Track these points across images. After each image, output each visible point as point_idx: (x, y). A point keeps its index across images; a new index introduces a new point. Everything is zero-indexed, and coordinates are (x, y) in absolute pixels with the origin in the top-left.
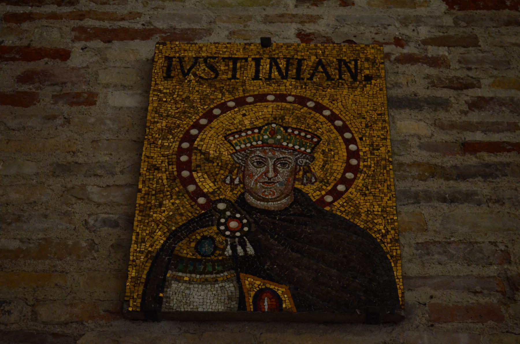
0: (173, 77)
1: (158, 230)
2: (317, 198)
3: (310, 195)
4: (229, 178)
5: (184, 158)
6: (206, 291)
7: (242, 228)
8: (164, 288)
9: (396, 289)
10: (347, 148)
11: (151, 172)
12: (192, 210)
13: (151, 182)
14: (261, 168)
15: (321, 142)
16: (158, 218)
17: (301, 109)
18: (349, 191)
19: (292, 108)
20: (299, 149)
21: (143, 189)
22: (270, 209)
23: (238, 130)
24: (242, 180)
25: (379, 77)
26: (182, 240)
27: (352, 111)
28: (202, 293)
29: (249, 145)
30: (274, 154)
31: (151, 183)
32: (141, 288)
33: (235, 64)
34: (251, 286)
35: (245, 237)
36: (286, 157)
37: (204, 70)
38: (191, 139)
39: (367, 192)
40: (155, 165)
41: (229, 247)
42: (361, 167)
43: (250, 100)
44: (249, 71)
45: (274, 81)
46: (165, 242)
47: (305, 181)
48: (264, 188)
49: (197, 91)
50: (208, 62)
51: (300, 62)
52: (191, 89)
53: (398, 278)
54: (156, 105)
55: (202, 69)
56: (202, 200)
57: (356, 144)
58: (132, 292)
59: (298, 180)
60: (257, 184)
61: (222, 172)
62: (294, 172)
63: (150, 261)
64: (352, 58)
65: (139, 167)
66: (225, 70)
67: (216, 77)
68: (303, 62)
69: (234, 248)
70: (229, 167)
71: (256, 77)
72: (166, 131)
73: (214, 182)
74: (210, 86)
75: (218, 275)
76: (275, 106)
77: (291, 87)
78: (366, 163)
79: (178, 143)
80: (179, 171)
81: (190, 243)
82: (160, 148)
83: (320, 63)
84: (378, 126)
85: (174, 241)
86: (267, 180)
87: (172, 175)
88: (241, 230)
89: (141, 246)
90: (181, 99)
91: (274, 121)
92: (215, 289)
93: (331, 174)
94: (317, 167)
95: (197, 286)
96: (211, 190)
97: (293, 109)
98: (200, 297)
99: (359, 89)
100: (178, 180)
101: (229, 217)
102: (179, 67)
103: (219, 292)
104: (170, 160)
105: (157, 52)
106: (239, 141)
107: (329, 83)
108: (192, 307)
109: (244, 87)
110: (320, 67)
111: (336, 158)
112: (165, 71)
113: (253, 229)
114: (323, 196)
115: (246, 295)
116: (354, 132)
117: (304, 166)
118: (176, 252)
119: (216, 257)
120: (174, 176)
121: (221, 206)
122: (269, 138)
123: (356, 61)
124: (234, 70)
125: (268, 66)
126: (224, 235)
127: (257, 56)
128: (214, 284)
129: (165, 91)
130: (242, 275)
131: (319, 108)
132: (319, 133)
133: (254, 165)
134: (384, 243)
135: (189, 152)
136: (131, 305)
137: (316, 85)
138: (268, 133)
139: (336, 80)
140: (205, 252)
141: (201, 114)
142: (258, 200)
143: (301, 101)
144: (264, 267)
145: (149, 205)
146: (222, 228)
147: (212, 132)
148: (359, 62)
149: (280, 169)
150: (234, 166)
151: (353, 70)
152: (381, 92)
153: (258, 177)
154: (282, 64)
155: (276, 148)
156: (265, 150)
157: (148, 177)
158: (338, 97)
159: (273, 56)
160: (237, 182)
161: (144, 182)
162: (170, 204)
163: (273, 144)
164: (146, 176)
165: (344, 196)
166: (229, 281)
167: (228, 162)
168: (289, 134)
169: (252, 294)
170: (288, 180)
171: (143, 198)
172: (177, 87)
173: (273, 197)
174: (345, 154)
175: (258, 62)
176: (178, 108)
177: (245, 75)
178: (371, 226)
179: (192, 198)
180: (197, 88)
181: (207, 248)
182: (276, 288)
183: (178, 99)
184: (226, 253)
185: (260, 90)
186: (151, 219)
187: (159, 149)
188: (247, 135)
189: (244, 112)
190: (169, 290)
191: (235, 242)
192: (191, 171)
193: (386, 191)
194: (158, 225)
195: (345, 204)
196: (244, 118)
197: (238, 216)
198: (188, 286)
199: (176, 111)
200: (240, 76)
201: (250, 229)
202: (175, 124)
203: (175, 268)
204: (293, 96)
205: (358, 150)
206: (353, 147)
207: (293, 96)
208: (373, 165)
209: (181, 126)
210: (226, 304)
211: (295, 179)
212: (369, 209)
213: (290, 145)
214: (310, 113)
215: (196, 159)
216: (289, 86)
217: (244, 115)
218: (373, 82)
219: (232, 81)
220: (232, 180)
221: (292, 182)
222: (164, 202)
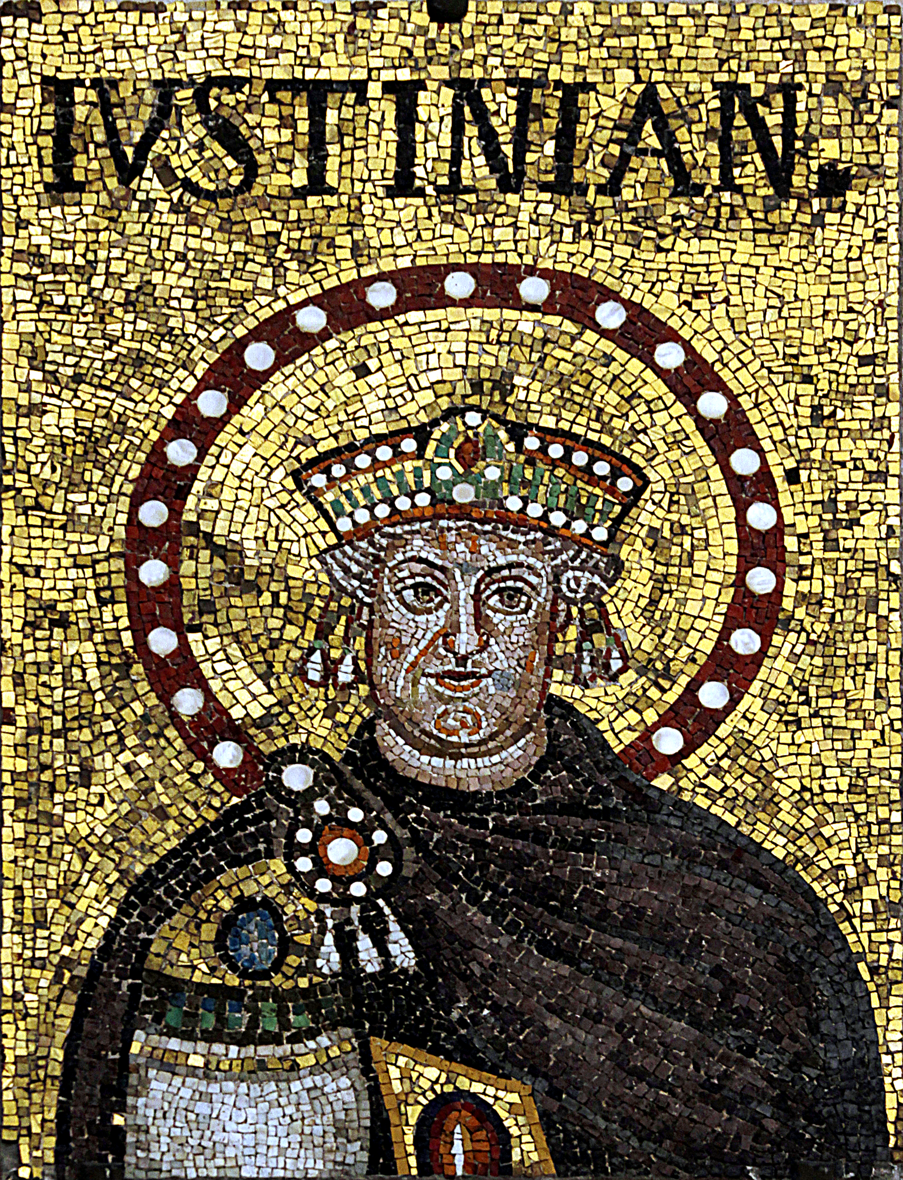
0: (80, 187)
2: (628, 737)
4: (317, 657)
5: (153, 572)
8: (124, 1095)
10: (741, 521)
11: (39, 634)
13: (44, 678)
14: (429, 611)
15: (646, 495)
18: (741, 707)
20: (567, 525)
23: (344, 440)
26: (170, 913)
29: (383, 511)
32: (53, 1097)
35: (381, 902)
39: (804, 711)
41: (329, 939)
42: (788, 604)
43: (382, 296)
45: (471, 198)
46: (116, 923)
49: (181, 257)
50: (213, 104)
53: (889, 1052)
56: (227, 754)
60: (415, 683)
61: (292, 632)
62: (549, 629)
66: (279, 145)
71: (403, 185)
75: (298, 1048)
76: (476, 324)
78: (804, 586)
79: (125, 503)
80: (140, 632)
81: (198, 927)
82: (63, 527)
83: (648, 104)
84: (858, 413)
87: (115, 649)
88: (367, 874)
90: (120, 296)
91: (474, 400)
92: (293, 1098)
96: (257, 712)
97: (545, 341)
101: (326, 819)
104: (104, 581)
106: (348, 494)
107: (684, 210)
108: (220, 1162)
110: (648, 126)
111: (699, 568)
115: (394, 1119)
116: (767, 445)
118: (154, 963)
121: (296, 777)
127: (404, 75)
129: (57, 257)
130: (377, 1043)
131: (642, 333)
132: (636, 454)
134: (849, 918)
136: (25, 1159)
137: (634, 222)
138: (452, 452)
139: (708, 191)
143: (576, 297)
144: (448, 1013)
145: (47, 776)
147: (246, 453)
148: (801, 95)
149: (497, 618)
152: (880, 250)
153: (422, 653)
155: (482, 522)
157: (30, 658)
158: (715, 278)
160: (345, 675)
165: (723, 730)
167: (312, 589)
169: (414, 1113)
172: (103, 236)
173: (475, 738)
174: (733, 546)
176: (114, 341)
179: (191, 746)
181: (257, 947)
182: (491, 1091)
186: (59, 831)
187: (59, 534)
190: (141, 1101)
191: (349, 922)
192: (181, 629)
195: (725, 763)
197: (355, 815)
201: (397, 867)
204: (545, 274)
205: (780, 528)
206: (761, 516)
207: (545, 274)
209: (132, 423)
212: (807, 782)
213: (535, 510)
214: (609, 359)
216: (530, 230)
218: (852, 197)
219: (312, 201)
220: (330, 668)
221: (542, 673)
222: (98, 763)
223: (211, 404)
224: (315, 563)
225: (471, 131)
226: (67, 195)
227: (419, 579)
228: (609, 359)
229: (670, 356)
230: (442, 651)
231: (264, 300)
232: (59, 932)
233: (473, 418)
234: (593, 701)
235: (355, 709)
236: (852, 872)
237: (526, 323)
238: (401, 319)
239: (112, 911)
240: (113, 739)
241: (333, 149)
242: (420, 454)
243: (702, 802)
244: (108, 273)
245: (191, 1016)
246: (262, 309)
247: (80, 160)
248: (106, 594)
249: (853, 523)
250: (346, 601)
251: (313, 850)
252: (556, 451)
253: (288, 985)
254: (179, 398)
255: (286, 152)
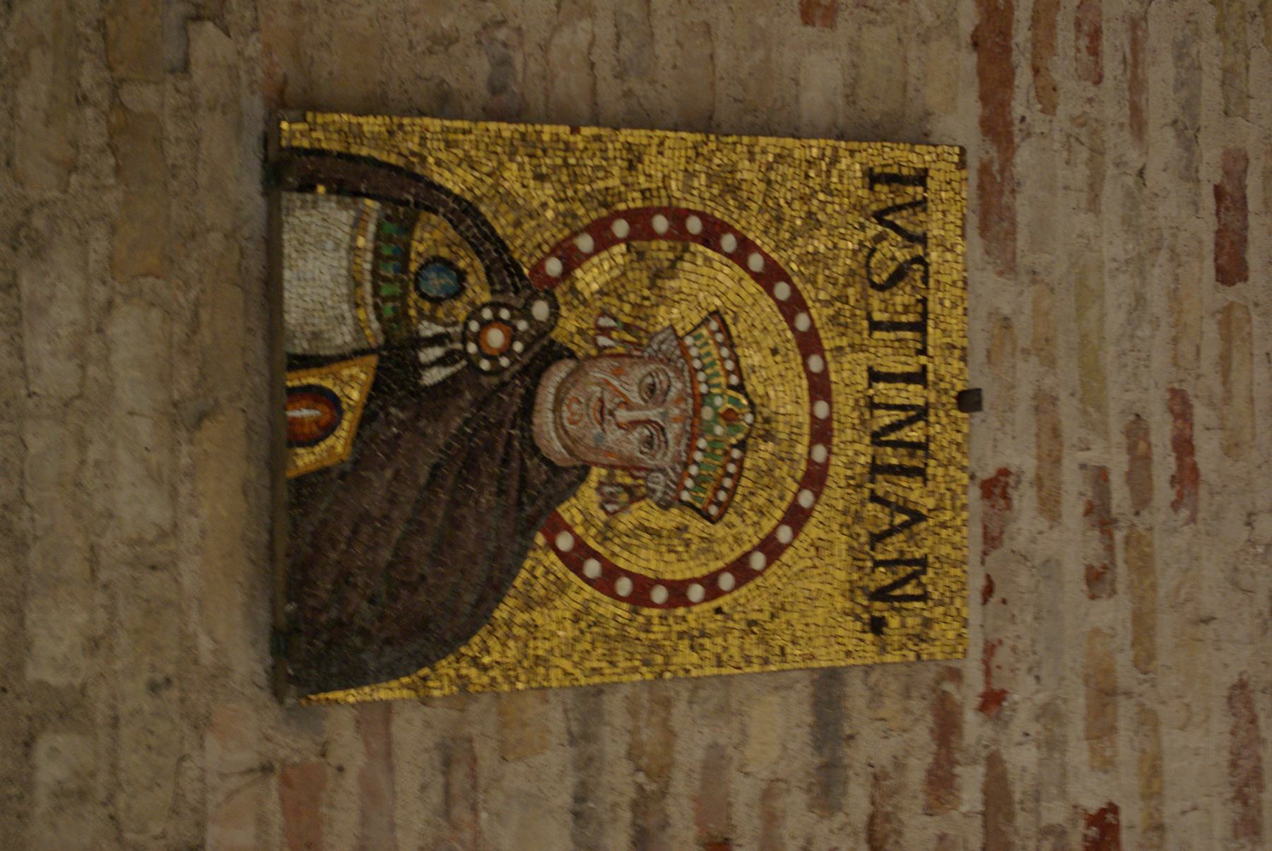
0: (871, 189)
1: (477, 174)
2: (566, 517)
3: (573, 501)
4: (612, 323)
5: (660, 224)
6: (331, 285)
7: (489, 357)
8: (338, 192)
9: (346, 687)
11: (624, 152)
12: (529, 246)
16: (506, 174)
17: (793, 477)
19: (796, 457)
20: (690, 476)
21: (579, 138)
22: (536, 414)
23: (736, 341)
24: (607, 352)
25: (883, 650)
26: (455, 228)
27: (790, 589)
28: (327, 277)
29: (697, 364)
30: (675, 420)
31: (594, 154)
32: (335, 146)
33: (910, 327)
34: (346, 378)
35: (464, 363)
36: (667, 447)
37: (893, 259)
38: (711, 236)
39: (583, 625)
40: (640, 161)
41: (440, 329)
42: (646, 611)
43: (815, 364)
44: (892, 358)
45: (867, 416)
46: (449, 193)
47: (607, 489)
48: (589, 400)
49: (835, 246)
50: (915, 266)
51: (920, 472)
52: (842, 231)
54: (796, 156)
55: (894, 251)
56: (554, 267)
57: (706, 599)
58: (325, 127)
59: (611, 476)
60: (598, 384)
61: (627, 308)
62: (631, 467)
63: (401, 163)
64: (930, 588)
65: (633, 125)
66: (894, 305)
67: (874, 285)
68: (919, 479)
69: (437, 340)
70: (638, 323)
72: (730, 182)
73: (601, 292)
74: (852, 273)
75: (370, 309)
76: (801, 419)
77: (850, 453)
78: (656, 621)
79: (700, 208)
80: (628, 215)
81: (448, 246)
82: (686, 170)
83: (917, 517)
85: (453, 211)
86: (608, 406)
87: (616, 199)
88: (482, 354)
89: (439, 140)
90: (814, 209)
91: (759, 419)
93: (626, 547)
94: (643, 514)
95: (345, 263)
96: (580, 286)
97: (792, 460)
98: (317, 272)
99: (848, 605)
100: (604, 212)
101: (515, 329)
102: (899, 201)
103: (331, 313)
104: (655, 193)
105: (939, 150)
108: (294, 255)
109: (848, 350)
110: (905, 517)
112: (887, 170)
113: (484, 381)
114: (569, 529)
115: (324, 370)
116: (736, 594)
117: (648, 488)
118: (424, 215)
119: (415, 302)
120: (613, 204)
121: (540, 310)
122: (715, 408)
123: (924, 597)
124: (894, 326)
125: (906, 402)
126: (469, 318)
127: (931, 377)
128: (349, 302)
129: (835, 172)
130: (373, 360)
131: (796, 517)
132: (731, 517)
133: (645, 376)
134: (458, 661)
135: (678, 233)
138: (729, 406)
140: (426, 279)
141: (774, 256)
142: (558, 390)
143: (815, 478)
144: (395, 406)
145: (539, 153)
146: (487, 314)
147: (729, 283)
150: (642, 334)
151: (897, 592)
152: (842, 655)
153: (617, 390)
154: (913, 434)
155: (692, 425)
156: (685, 400)
157: (610, 146)
159: (932, 412)
160: (603, 341)
161: (598, 138)
162: (543, 199)
163: (700, 418)
164: (612, 142)
165: (572, 576)
166: (357, 331)
167: (652, 321)
168: (726, 453)
169: (328, 384)
170: (609, 452)
171: (556, 138)
172: (846, 200)
174: (679, 577)
175: (919, 377)
176: (789, 204)
177: (882, 351)
178: (499, 633)
179: (559, 245)
180: (842, 244)
181: (436, 283)
182: (343, 434)
183: (815, 202)
184: (425, 323)
185: (841, 385)
186: (505, 158)
187: (682, 167)
188: (723, 359)
189: (782, 351)
190: (334, 205)
191: (452, 341)
192: (627, 240)
193: (588, 665)
194: (489, 175)
196: (768, 352)
197: (518, 347)
198: (344, 245)
199: (782, 202)
200: (877, 340)
202: (749, 199)
203: (388, 218)
204: (828, 459)
205: (689, 604)
206: (696, 592)
207: (828, 459)
208: (652, 636)
209: (744, 213)
210: (302, 328)
211: (611, 467)
213: (698, 456)
215: (659, 250)
216: (851, 452)
217: (775, 352)
218: (869, 637)
219: (865, 324)
220: (605, 331)
221: (605, 462)
222: (548, 185)
223: (756, 262)
224: (666, 324)
225: (902, 415)
226: (867, 180)
227: (658, 386)
228: (782, 498)
229: (785, 534)
230: (617, 400)
231: (813, 295)
232: (443, 156)
233: (749, 418)
234: (588, 495)
235: (582, 347)
236: (486, 660)
237: (801, 449)
238: (803, 375)
239: (457, 191)
240: (562, 195)
241: (892, 335)
242: (731, 387)
243: (528, 564)
244: (825, 203)
245: (389, 239)
246: (808, 292)
247: (885, 189)
248: (648, 194)
249: (692, 648)
250: (645, 341)
251: (497, 319)
252: (732, 468)
253: (411, 303)
254: (758, 242)
255: (891, 309)
